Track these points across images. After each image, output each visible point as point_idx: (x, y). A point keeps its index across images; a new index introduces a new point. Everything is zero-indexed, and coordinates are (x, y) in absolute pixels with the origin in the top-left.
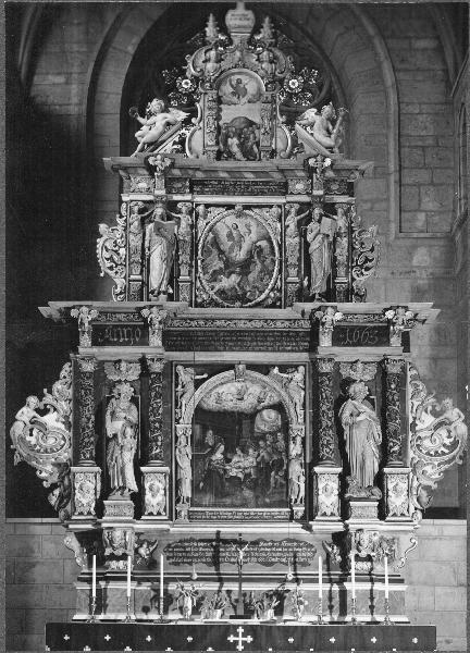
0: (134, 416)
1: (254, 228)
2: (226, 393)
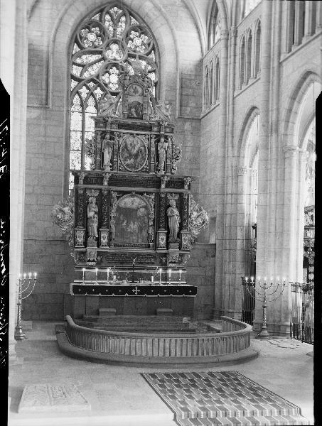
0: (97, 210)
1: (139, 143)
2: (127, 202)
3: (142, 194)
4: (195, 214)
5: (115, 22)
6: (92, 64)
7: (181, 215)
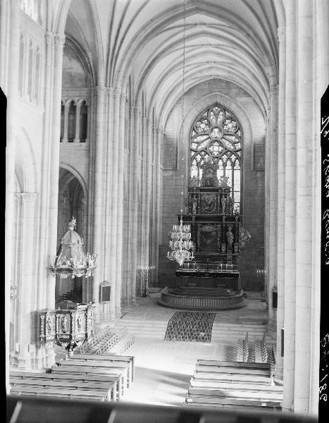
2: (207, 228)
3: (213, 224)
4: (243, 234)
5: (216, 115)
6: (203, 141)
7: (234, 235)
